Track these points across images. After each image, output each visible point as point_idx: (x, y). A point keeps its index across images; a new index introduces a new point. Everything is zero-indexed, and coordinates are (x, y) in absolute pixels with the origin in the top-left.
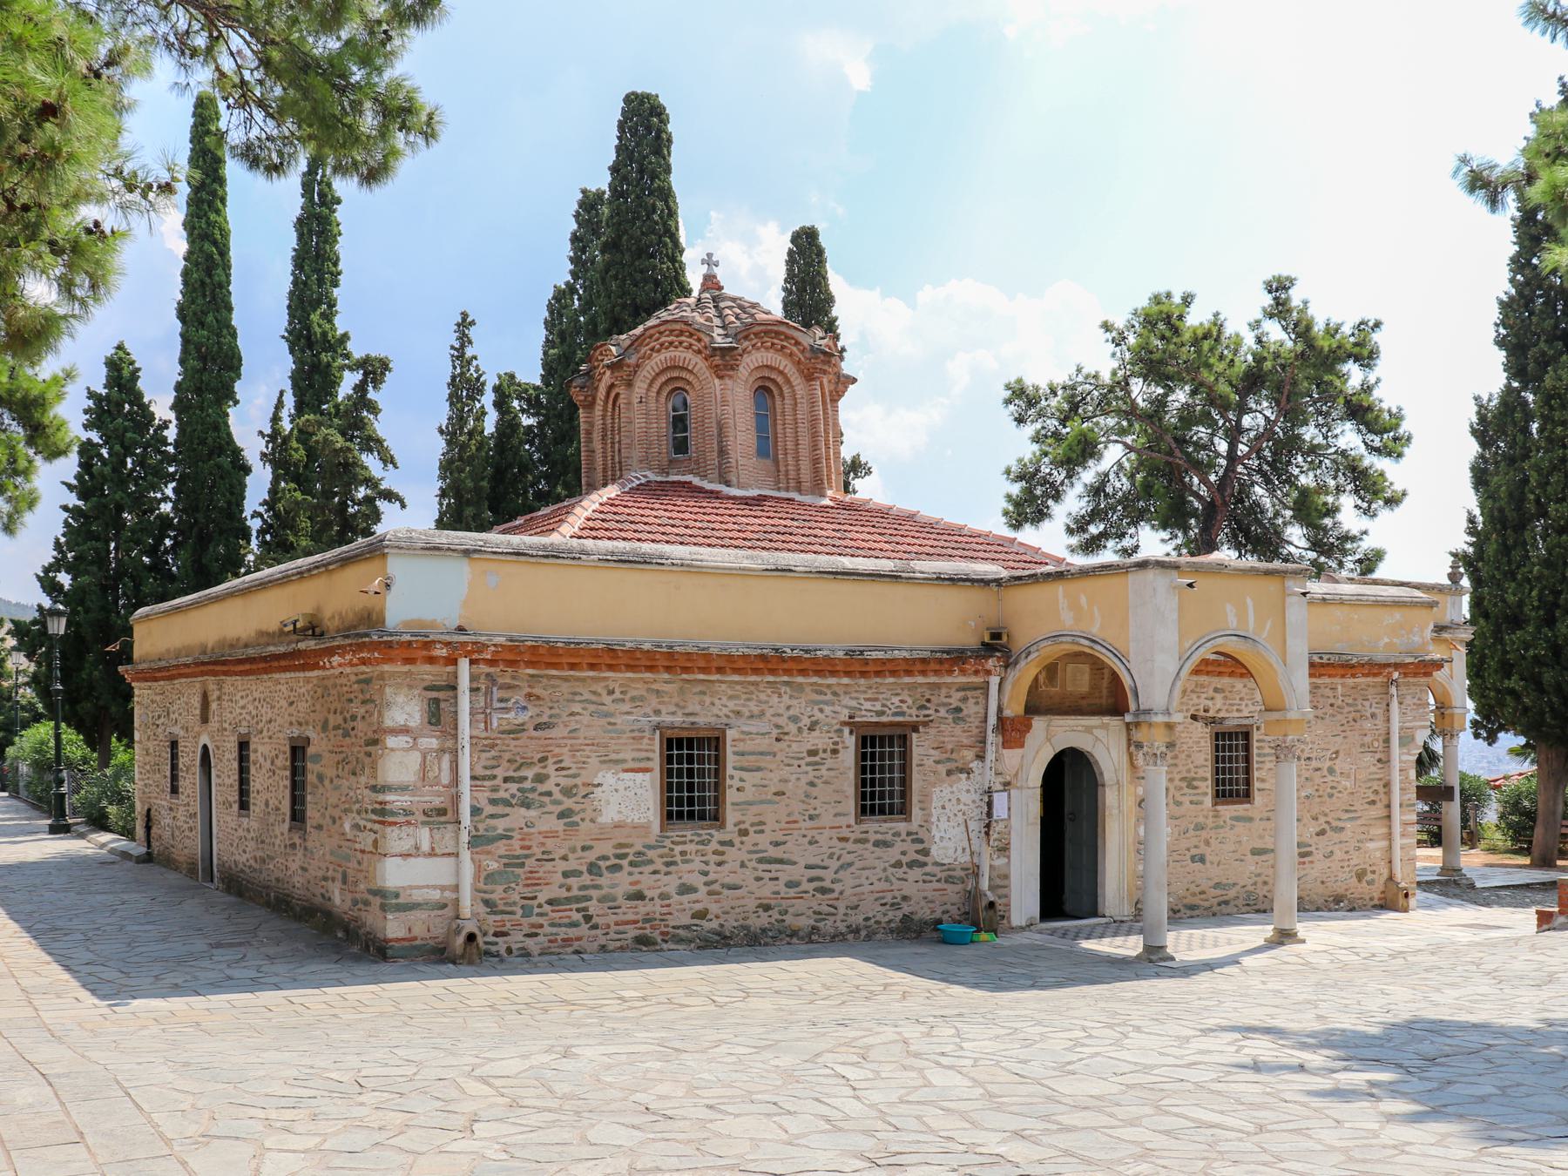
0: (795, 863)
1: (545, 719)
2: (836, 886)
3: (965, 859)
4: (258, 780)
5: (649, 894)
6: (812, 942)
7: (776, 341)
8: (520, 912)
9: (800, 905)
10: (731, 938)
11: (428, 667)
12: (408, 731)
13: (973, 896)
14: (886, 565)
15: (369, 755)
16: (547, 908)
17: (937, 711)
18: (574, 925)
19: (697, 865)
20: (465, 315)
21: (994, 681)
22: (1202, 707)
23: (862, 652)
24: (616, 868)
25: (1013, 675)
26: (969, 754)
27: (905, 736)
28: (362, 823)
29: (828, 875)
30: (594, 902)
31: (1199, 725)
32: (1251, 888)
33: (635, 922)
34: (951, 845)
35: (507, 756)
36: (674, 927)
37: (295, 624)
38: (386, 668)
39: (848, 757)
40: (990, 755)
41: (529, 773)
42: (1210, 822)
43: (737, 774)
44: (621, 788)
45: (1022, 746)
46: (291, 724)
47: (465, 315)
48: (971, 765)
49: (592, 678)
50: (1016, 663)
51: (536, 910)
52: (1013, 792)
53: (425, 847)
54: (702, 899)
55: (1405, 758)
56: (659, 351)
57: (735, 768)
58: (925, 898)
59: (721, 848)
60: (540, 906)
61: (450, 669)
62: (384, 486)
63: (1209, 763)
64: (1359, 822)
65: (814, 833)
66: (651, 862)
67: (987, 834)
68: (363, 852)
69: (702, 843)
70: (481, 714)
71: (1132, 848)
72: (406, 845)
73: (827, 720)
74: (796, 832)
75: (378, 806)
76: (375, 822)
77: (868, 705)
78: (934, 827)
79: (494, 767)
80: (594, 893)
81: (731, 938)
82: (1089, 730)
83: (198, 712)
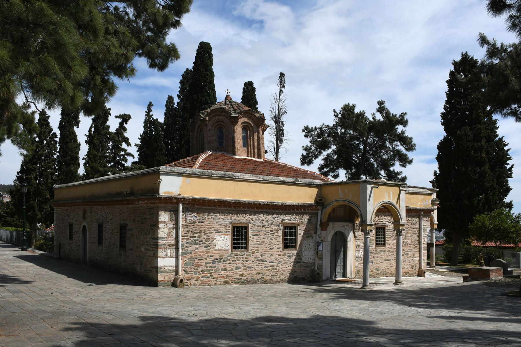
0: (267, 261)
1: (201, 220)
2: (278, 268)
3: (311, 261)
4: (106, 236)
5: (228, 269)
6: (271, 283)
7: (249, 115)
8: (194, 274)
9: (268, 273)
10: (249, 282)
11: (170, 205)
12: (164, 223)
13: (313, 271)
14: (291, 180)
15: (152, 229)
16: (201, 272)
17: (304, 220)
18: (208, 278)
19: (241, 261)
20: (151, 103)
21: (320, 212)
23: (286, 203)
24: (220, 262)
25: (324, 211)
26: (312, 232)
27: (296, 227)
28: (149, 248)
29: (275, 264)
30: (213, 271)
32: (385, 270)
33: (224, 277)
34: (307, 257)
35: (191, 230)
36: (234, 279)
37: (127, 192)
38: (160, 205)
39: (281, 232)
40: (318, 233)
41: (197, 235)
42: (374, 252)
43: (252, 236)
44: (221, 240)
45: (326, 230)
46: (120, 220)
47: (151, 103)
48: (313, 235)
49: (214, 209)
50: (326, 207)
51: (198, 273)
53: (169, 255)
54: (241, 271)
55: (424, 235)
56: (215, 116)
57: (251, 235)
58: (300, 272)
59: (247, 257)
60: (199, 272)
61: (176, 205)
62: (128, 152)
63: (374, 236)
64: (412, 252)
65: (272, 253)
66: (229, 260)
67: (317, 254)
68: (149, 256)
69: (242, 255)
70: (185, 219)
71: (354, 259)
72: (164, 253)
73: (276, 222)
74: (267, 253)
75: (155, 244)
76: (154, 248)
77: (286, 218)
78: (303, 252)
79: (187, 233)
80: (213, 269)
81: (249, 282)
82: (343, 226)
83: (82, 216)
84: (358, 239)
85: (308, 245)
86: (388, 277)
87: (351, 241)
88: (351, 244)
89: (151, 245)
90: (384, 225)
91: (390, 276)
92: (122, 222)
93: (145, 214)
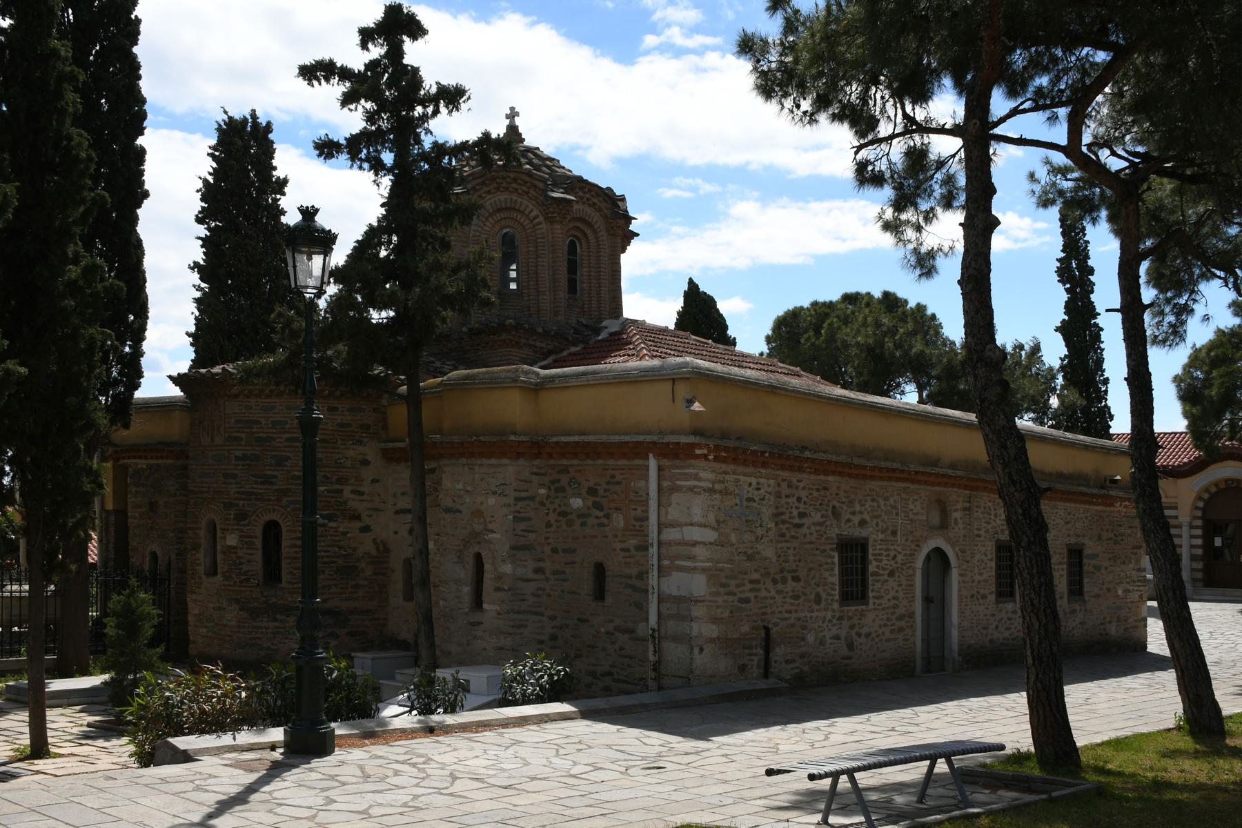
15: (1136, 554)
28: (1131, 588)
76: (1139, 586)
89: (1134, 581)
92: (1073, 540)
93: (1120, 526)
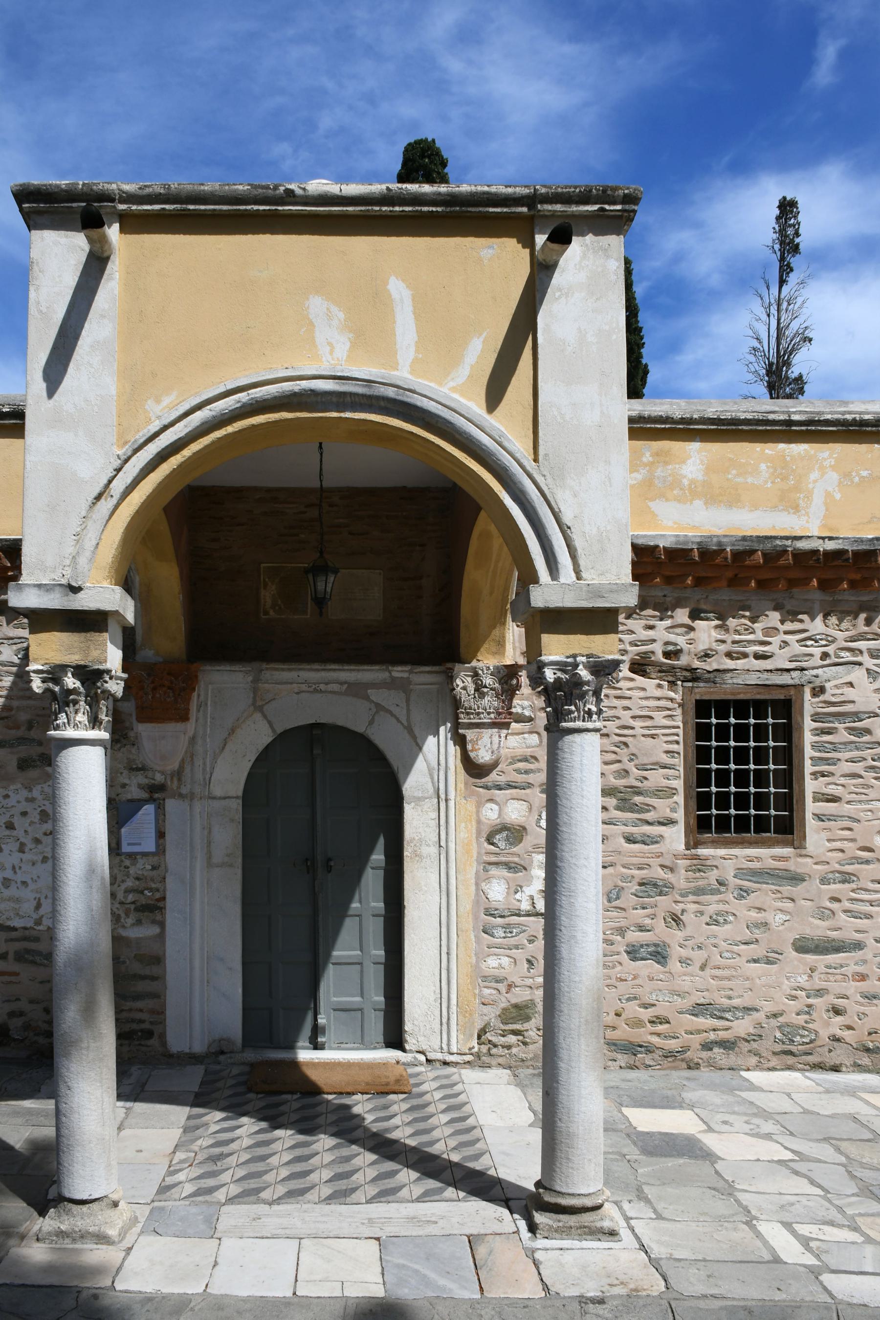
22: (658, 648)
31: (650, 684)
34: (28, 894)
52: (171, 805)
63: (679, 762)
71: (468, 924)
82: (357, 690)
84: (510, 786)
85: (35, 816)
86: (836, 1069)
87: (440, 797)
88: (442, 824)
90: (785, 679)
91: (859, 1068)
